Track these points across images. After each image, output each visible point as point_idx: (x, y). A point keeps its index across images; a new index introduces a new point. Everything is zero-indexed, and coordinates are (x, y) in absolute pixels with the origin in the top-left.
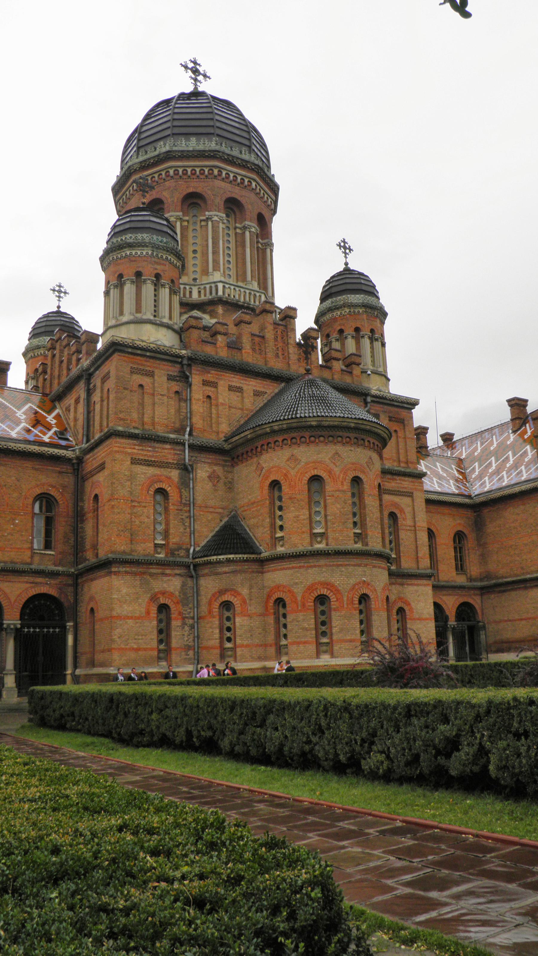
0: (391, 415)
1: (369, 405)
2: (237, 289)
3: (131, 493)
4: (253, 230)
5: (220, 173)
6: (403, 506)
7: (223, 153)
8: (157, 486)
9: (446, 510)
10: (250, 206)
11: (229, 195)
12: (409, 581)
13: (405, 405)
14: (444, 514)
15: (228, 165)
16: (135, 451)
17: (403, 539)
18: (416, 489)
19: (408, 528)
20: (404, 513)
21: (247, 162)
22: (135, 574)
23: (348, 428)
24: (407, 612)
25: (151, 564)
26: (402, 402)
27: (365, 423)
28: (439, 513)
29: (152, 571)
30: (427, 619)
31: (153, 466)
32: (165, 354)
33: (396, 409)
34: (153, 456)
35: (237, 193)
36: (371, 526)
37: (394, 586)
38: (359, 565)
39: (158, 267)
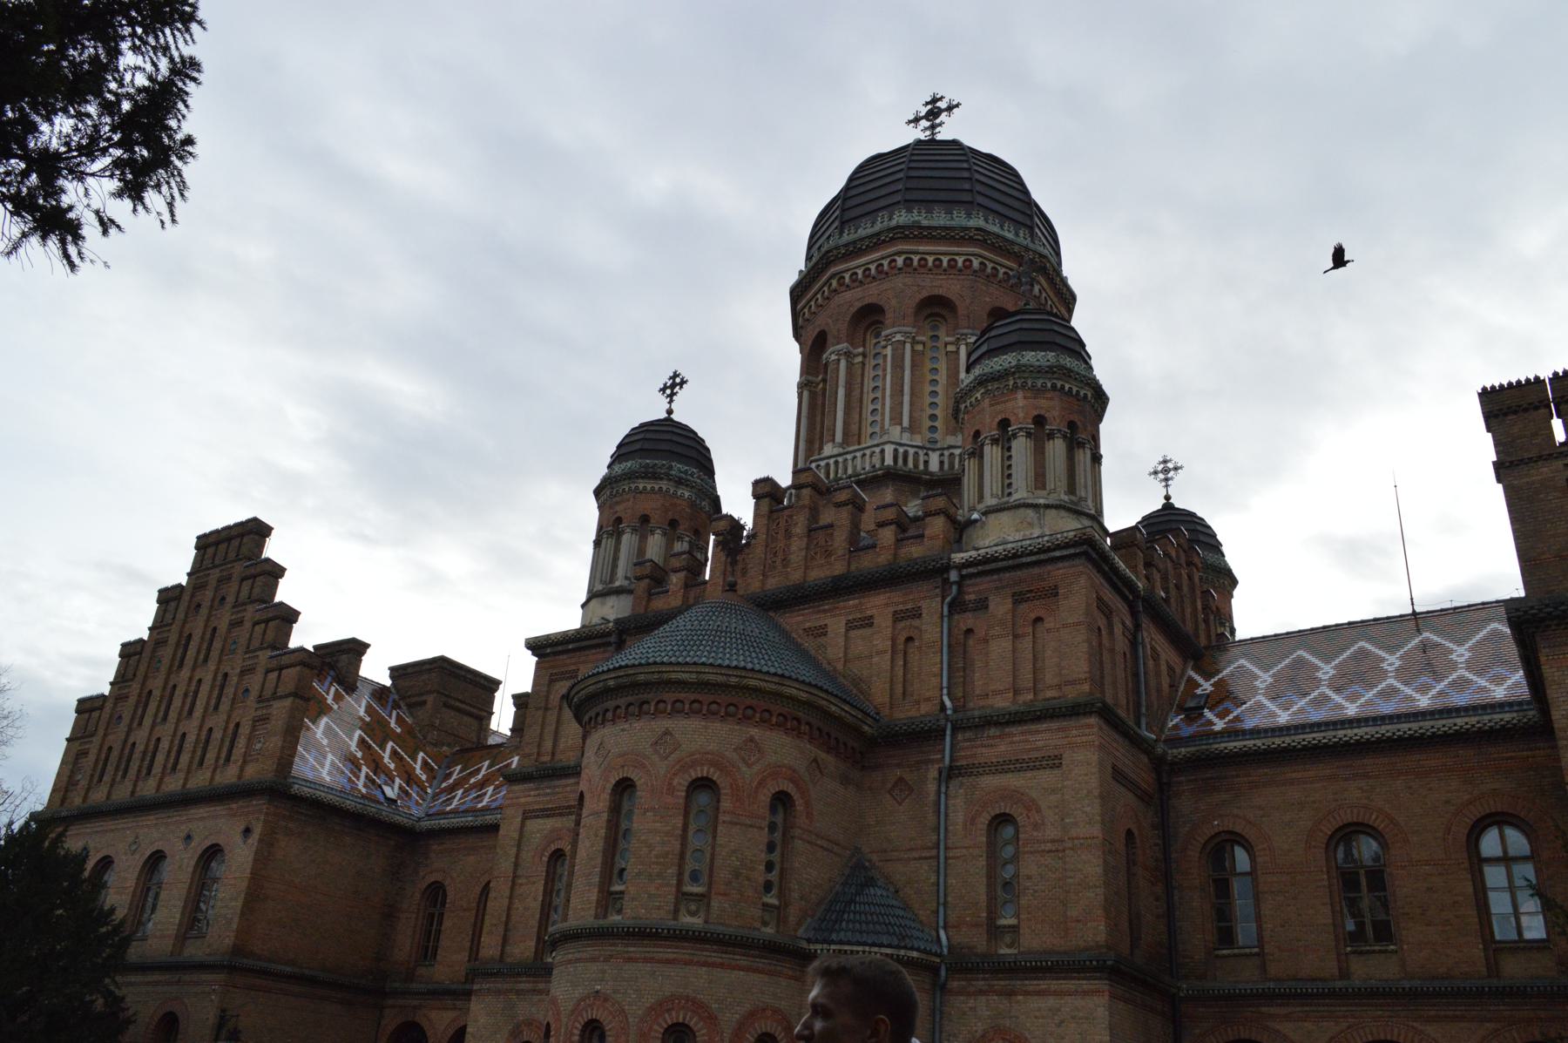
0: (1017, 589)
2: (840, 459)
3: (516, 865)
4: (898, 337)
6: (1034, 795)
8: (553, 847)
10: (894, 302)
11: (858, 305)
12: (1032, 985)
13: (1057, 554)
15: (853, 259)
16: (530, 799)
17: (1029, 877)
19: (1049, 846)
20: (1039, 811)
22: (499, 992)
23: (607, 692)
25: (519, 975)
26: (1041, 551)
27: (631, 672)
29: (522, 986)
31: (553, 815)
33: (1036, 570)
35: (871, 293)
36: (639, 874)
37: (983, 998)
38: (594, 960)
39: (618, 508)
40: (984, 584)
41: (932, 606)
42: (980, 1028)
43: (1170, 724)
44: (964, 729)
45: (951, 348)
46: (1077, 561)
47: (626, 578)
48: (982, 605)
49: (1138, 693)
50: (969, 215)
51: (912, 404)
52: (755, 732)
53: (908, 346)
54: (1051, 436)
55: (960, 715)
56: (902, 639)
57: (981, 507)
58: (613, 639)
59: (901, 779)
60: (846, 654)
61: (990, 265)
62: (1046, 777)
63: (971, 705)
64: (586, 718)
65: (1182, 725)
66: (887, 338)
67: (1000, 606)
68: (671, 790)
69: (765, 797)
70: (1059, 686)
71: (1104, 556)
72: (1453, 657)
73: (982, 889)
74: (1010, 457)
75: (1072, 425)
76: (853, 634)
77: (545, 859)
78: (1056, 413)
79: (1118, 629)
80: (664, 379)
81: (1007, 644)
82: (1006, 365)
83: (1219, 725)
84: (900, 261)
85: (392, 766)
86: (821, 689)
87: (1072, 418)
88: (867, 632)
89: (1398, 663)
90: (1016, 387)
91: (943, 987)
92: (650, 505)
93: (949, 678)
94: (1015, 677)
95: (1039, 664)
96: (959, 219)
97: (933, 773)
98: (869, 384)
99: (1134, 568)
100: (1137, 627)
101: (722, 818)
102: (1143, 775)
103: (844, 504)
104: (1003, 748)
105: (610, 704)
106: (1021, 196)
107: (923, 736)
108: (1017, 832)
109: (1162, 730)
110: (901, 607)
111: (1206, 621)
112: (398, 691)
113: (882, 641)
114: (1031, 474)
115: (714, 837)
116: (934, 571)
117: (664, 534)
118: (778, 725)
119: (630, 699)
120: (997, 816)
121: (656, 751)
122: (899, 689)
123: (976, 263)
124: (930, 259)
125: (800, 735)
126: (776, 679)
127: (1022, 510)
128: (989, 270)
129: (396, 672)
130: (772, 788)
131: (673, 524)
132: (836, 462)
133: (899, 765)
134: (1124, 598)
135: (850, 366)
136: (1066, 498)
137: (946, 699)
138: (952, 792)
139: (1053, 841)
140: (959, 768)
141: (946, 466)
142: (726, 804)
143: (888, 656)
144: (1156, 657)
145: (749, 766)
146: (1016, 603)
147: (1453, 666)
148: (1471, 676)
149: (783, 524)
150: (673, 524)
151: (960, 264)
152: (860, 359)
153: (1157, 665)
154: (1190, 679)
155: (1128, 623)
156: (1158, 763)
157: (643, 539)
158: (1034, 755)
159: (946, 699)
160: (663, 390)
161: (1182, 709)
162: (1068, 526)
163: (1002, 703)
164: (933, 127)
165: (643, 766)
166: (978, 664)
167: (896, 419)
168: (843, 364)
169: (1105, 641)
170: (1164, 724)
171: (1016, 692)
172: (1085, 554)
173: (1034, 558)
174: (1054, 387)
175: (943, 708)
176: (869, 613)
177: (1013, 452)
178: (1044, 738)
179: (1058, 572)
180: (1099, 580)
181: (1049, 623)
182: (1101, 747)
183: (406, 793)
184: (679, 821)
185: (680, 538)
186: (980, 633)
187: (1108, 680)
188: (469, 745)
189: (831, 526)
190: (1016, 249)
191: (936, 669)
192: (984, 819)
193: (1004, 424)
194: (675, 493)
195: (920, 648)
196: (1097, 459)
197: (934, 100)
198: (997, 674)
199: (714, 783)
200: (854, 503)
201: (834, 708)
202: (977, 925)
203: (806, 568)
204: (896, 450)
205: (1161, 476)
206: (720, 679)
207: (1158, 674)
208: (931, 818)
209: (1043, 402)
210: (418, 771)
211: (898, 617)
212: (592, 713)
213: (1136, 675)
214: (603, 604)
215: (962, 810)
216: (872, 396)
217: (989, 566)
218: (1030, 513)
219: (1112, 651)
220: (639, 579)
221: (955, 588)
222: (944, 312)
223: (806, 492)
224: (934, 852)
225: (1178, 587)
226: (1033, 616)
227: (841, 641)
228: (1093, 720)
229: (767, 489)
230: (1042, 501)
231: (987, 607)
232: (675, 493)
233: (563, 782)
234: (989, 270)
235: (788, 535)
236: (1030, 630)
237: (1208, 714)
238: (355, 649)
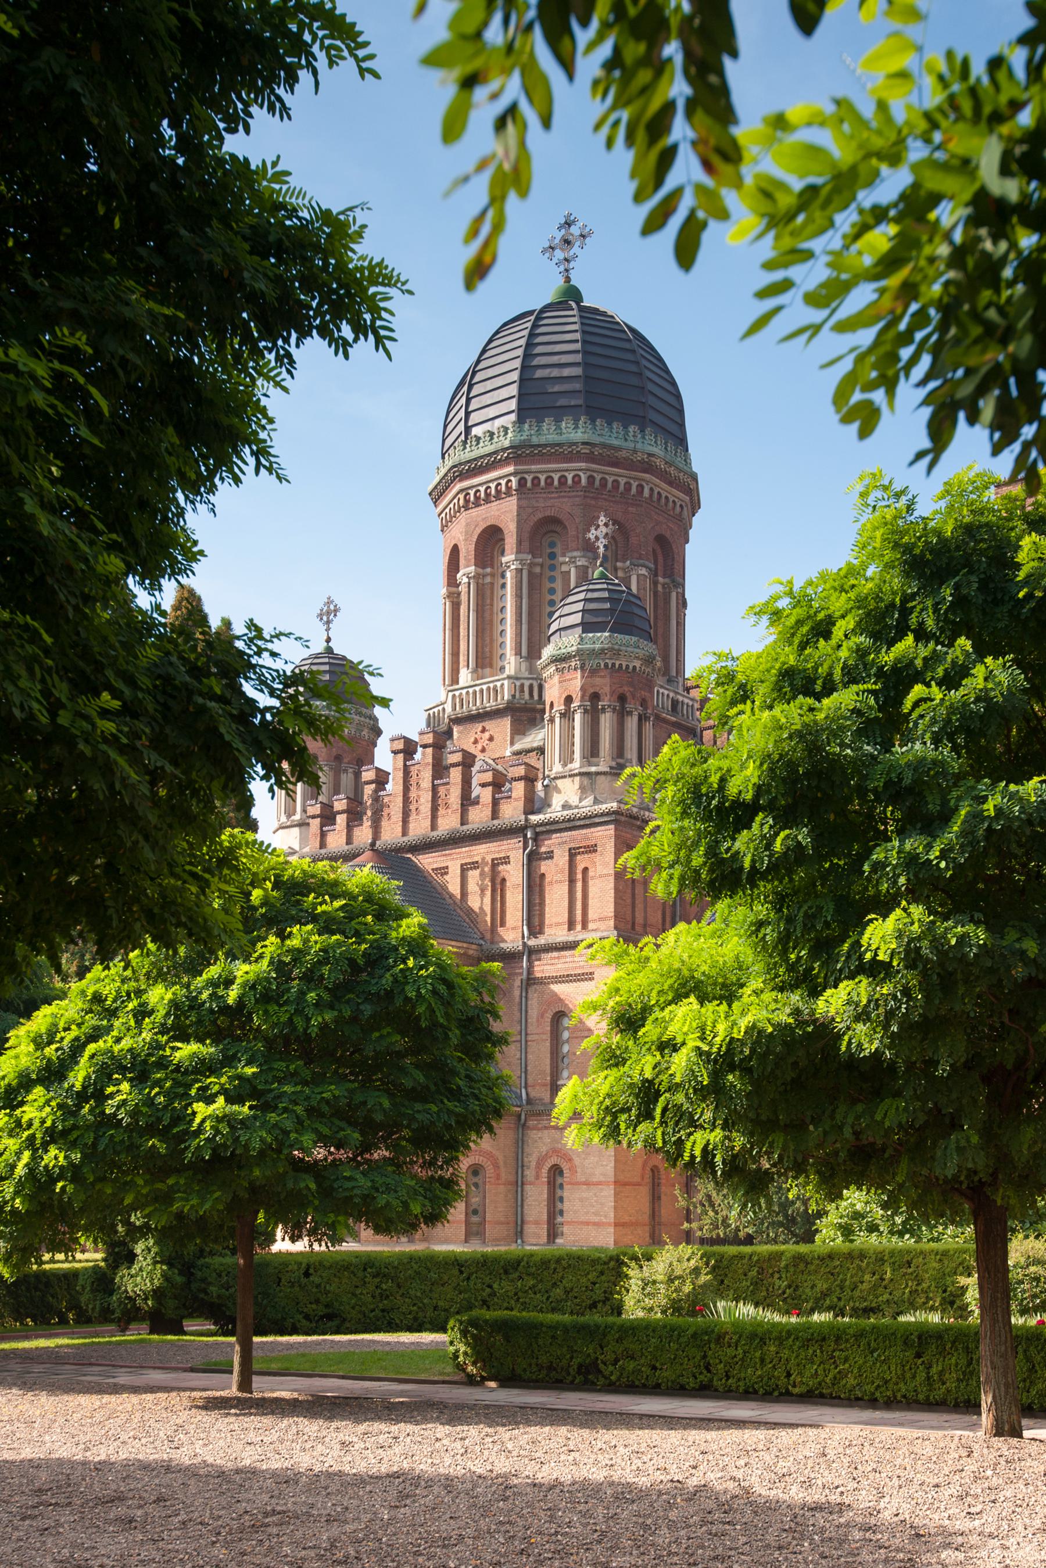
0: (573, 845)
7: (461, 464)
13: (597, 820)
24: (566, 1173)
26: (585, 818)
30: (599, 1183)
33: (584, 831)
42: (544, 1149)
48: (550, 855)
54: (603, 710)
61: (598, 477)
73: (548, 1062)
75: (622, 699)
78: (607, 689)
87: (621, 691)
91: (524, 1125)
97: (518, 983)
110: (497, 856)
123: (584, 481)
124: (543, 478)
128: (597, 483)
136: (614, 764)
138: (530, 996)
174: (606, 665)
190: (623, 454)
192: (549, 1016)
193: (569, 700)
202: (545, 1085)
209: (598, 681)
230: (593, 769)
234: (597, 483)
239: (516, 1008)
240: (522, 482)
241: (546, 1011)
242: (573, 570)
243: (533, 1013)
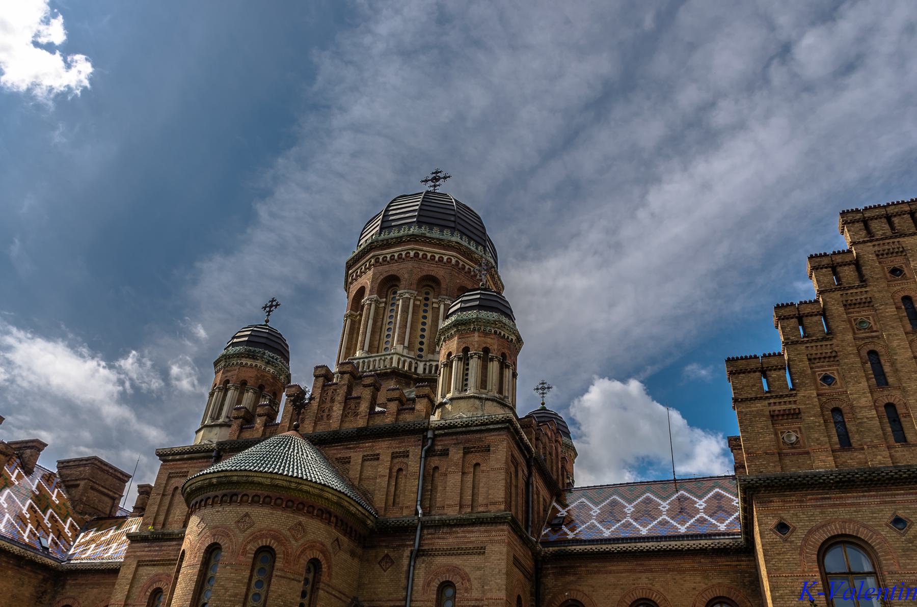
0: (467, 445)
1: (430, 441)
2: (366, 360)
3: (128, 597)
4: (407, 295)
5: (377, 260)
6: (467, 570)
8: (155, 586)
9: (686, 564)
10: (406, 276)
11: (386, 275)
13: (491, 427)
14: (682, 572)
16: (143, 553)
18: (492, 542)
20: (469, 580)
21: (401, 237)
26: (482, 424)
27: (229, 474)
28: (669, 570)
31: (158, 565)
32: (198, 452)
33: (478, 436)
34: (156, 556)
35: (394, 269)
39: (229, 374)
40: (447, 441)
41: (415, 451)
43: (543, 533)
44: (428, 527)
45: (435, 305)
46: (502, 433)
47: (227, 417)
48: (445, 453)
49: (527, 512)
50: (452, 235)
51: (410, 334)
52: (302, 519)
53: (412, 301)
54: (492, 360)
55: (427, 518)
56: (395, 469)
57: (449, 396)
58: (214, 454)
59: (387, 555)
60: (361, 475)
62: (475, 560)
63: (433, 512)
64: (193, 502)
65: (550, 534)
66: (401, 295)
67: (456, 454)
68: (245, 553)
69: (303, 561)
70: (487, 505)
71: (517, 432)
72: (697, 505)
74: (467, 369)
75: (503, 355)
76: (367, 463)
77: (148, 594)
78: (496, 347)
79: (520, 474)
80: (265, 301)
81: (458, 477)
82: (470, 317)
83: (571, 536)
84: (412, 254)
85: (49, 525)
86: (346, 495)
88: (376, 463)
89: (668, 507)
90: (474, 330)
92: (249, 375)
93: (422, 495)
94: (461, 498)
95: (476, 490)
96: (447, 235)
97: (407, 553)
98: (387, 320)
99: (530, 440)
100: (530, 474)
101: (275, 573)
102: (528, 564)
103: (368, 386)
104: (451, 540)
105: (211, 494)
106: (480, 229)
107: (403, 531)
108: (455, 593)
109: (539, 536)
110: (397, 450)
111: (563, 475)
112: (61, 475)
113: (383, 468)
114: (479, 380)
115: (269, 585)
116: (420, 431)
117: (255, 393)
118: (317, 515)
119: (225, 491)
120: (443, 582)
121: (238, 527)
122: (391, 498)
123: (454, 261)
125: (329, 523)
126: (320, 487)
127: (472, 400)
129: (63, 465)
130: (310, 555)
131: (261, 387)
132: (364, 362)
133: (387, 547)
134: (525, 456)
135: (377, 308)
136: (497, 395)
137: (419, 507)
138: (418, 566)
139: (476, 600)
140: (424, 551)
141: (427, 371)
142: (279, 564)
143: (387, 478)
144: (538, 494)
145: (296, 540)
146: (465, 454)
147: (697, 511)
148: (707, 517)
149: (330, 393)
150: (261, 387)
151: (445, 260)
152: (383, 305)
153: (538, 497)
154: (554, 508)
155: (525, 471)
156: (536, 555)
157: (241, 394)
158: (471, 546)
159: (419, 507)
160: (265, 308)
161: (550, 524)
162: (500, 413)
163: (452, 513)
164: (435, 186)
165: (228, 535)
166: (440, 488)
167: (401, 341)
168: (373, 306)
169: (514, 482)
170: (540, 533)
171: (461, 506)
172: (507, 428)
173: (478, 428)
174: (495, 332)
175: (417, 513)
176: (377, 452)
177: (470, 367)
178: (475, 536)
179: (490, 438)
180: (513, 444)
181: (483, 467)
182: (509, 544)
183: (56, 544)
184: (247, 574)
185: (264, 397)
186: (442, 470)
187: (513, 503)
188: (103, 515)
189: (359, 398)
191: (415, 489)
192: (435, 584)
193: (466, 350)
194: (265, 369)
195: (406, 475)
196: (515, 375)
197: (437, 173)
198: (450, 494)
199: (273, 550)
200: (374, 386)
201: (352, 508)
203: (342, 421)
204: (399, 359)
205: (541, 391)
206: (285, 483)
207: (538, 502)
208: (404, 581)
209: (489, 340)
210: (66, 530)
211: (394, 456)
212: (198, 499)
213: (527, 502)
214: (210, 432)
215: (423, 577)
216: (388, 327)
217: (450, 430)
218: (477, 402)
219: (516, 487)
220: (236, 418)
221: (430, 441)
222: (433, 285)
223: (346, 376)
224: (403, 603)
225: (550, 454)
226: (475, 462)
227: (359, 468)
228: (505, 527)
229: (323, 372)
230: (484, 396)
231: (448, 454)
232: (265, 369)
233: (168, 543)
235: (333, 400)
236: (472, 470)
237: (564, 528)
238: (37, 446)
239: (403, 576)
240: (416, 255)
241: (433, 580)
242: (442, 307)
243: (420, 581)
